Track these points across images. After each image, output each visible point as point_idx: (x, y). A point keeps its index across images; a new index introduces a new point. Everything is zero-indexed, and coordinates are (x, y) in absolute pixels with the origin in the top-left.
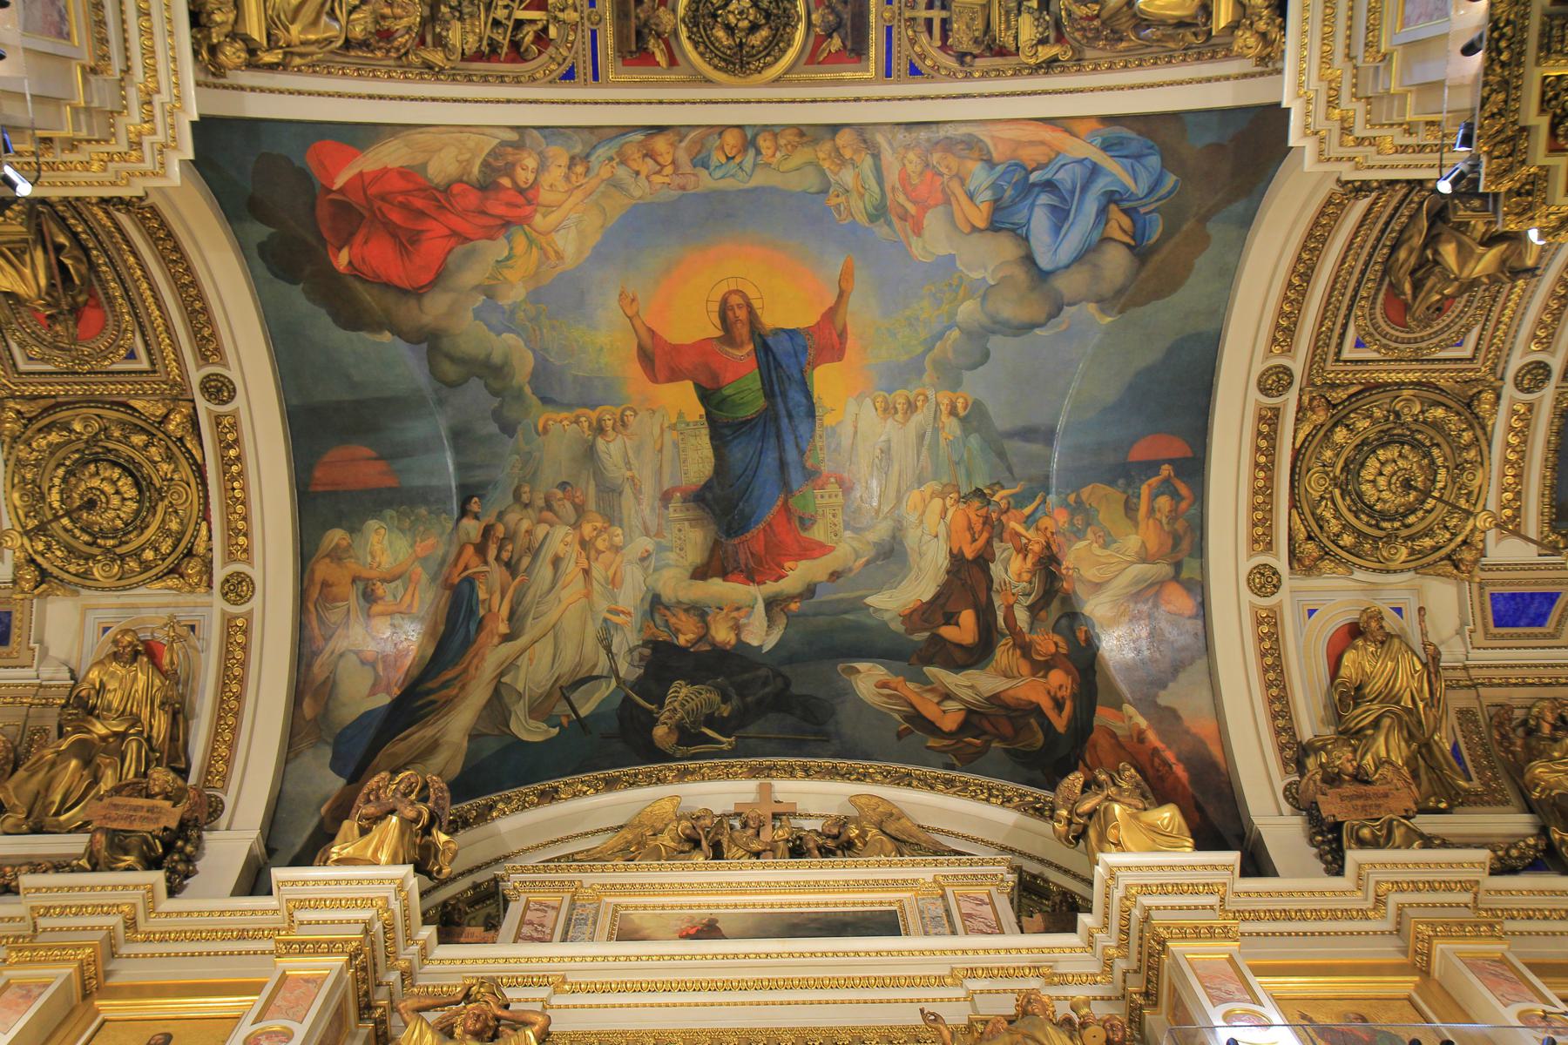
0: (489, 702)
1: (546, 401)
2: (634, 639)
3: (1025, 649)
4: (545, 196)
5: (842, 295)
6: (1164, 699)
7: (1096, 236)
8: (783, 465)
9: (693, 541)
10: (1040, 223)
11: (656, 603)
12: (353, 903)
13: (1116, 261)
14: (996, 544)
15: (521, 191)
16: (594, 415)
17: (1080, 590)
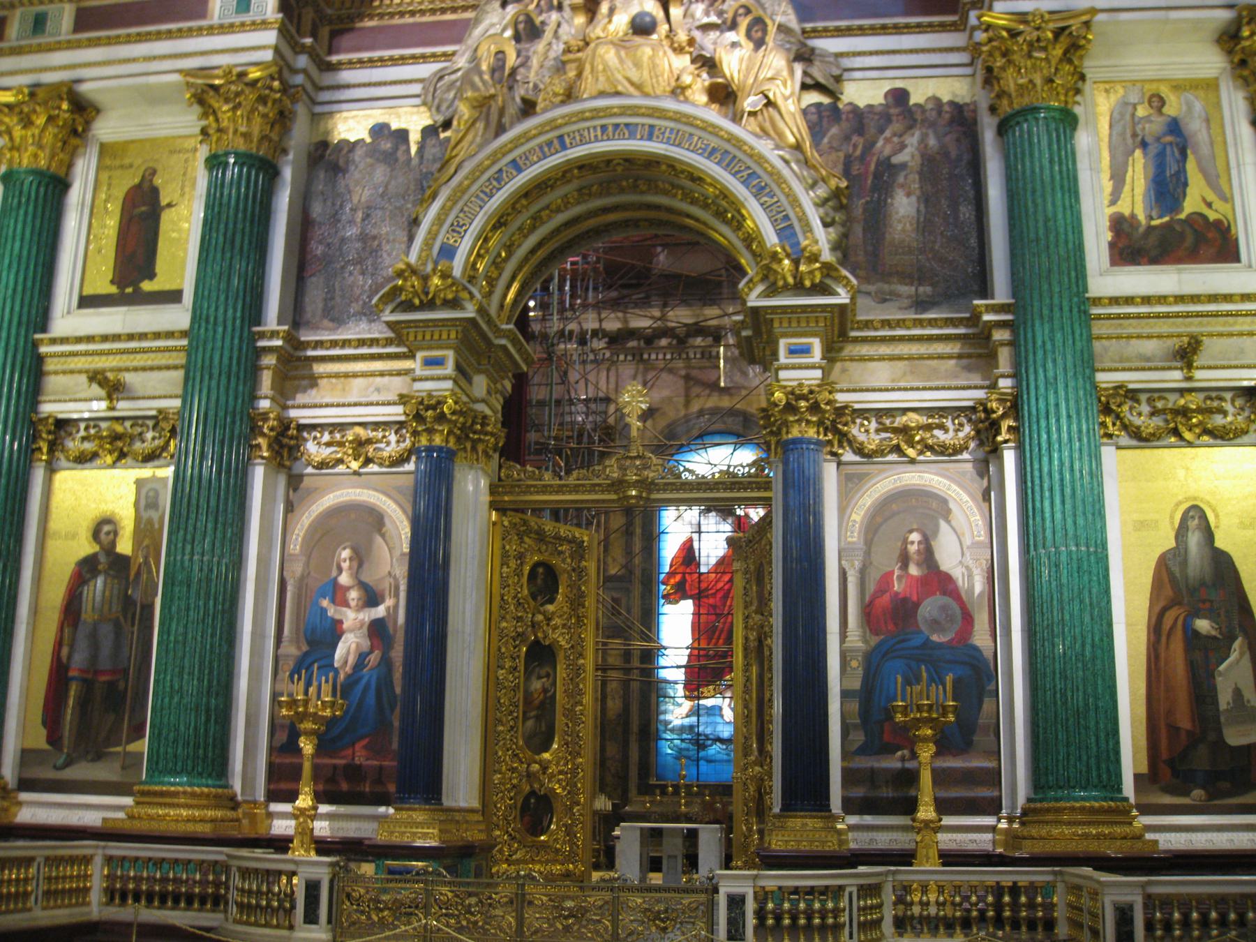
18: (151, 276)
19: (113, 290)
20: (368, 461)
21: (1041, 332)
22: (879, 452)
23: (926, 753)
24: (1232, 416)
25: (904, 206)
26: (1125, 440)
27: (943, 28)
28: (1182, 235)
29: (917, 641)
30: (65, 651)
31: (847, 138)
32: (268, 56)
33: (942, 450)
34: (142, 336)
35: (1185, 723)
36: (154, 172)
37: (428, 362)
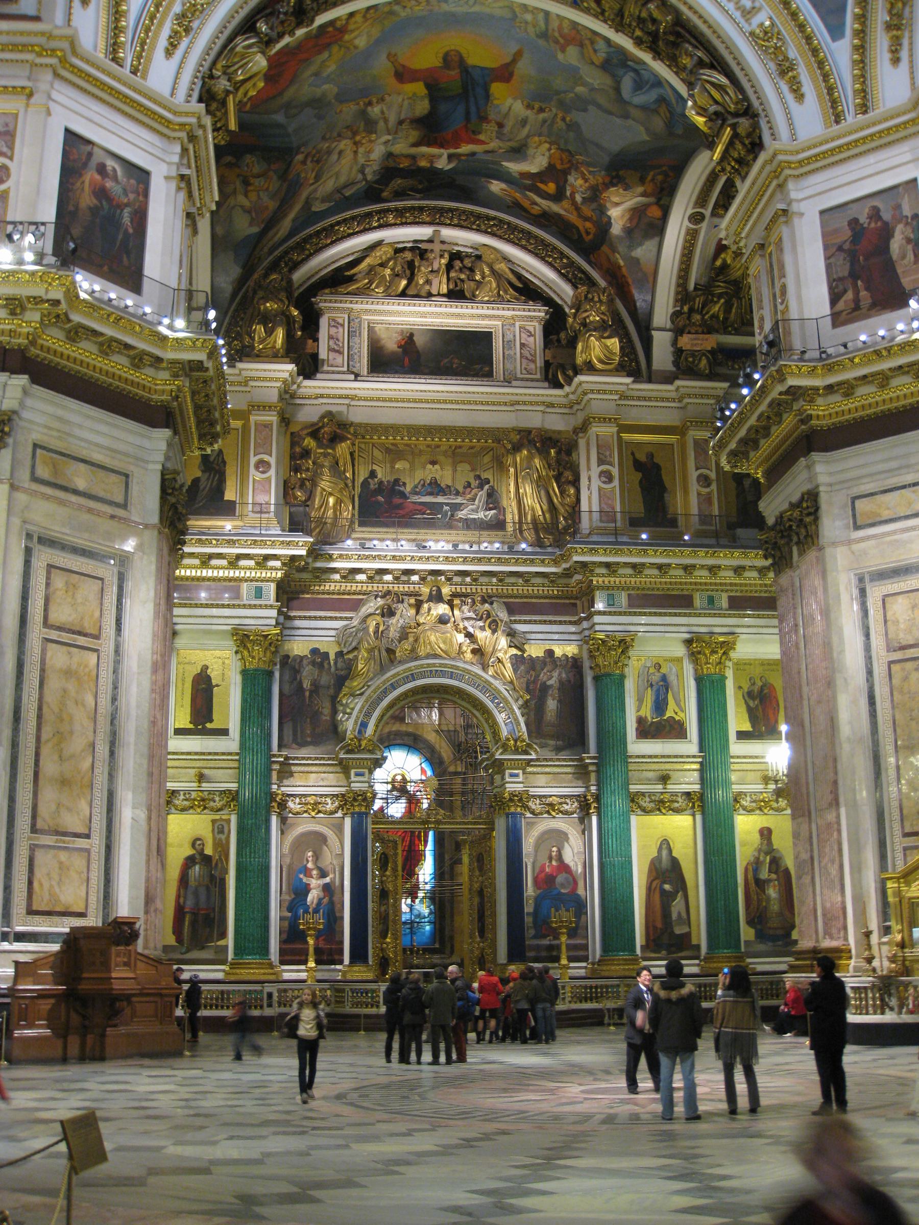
0: (302, 208)
1: (341, 102)
2: (376, 167)
3: (577, 209)
4: (351, 27)
5: (514, 61)
6: (634, 254)
7: (653, 107)
8: (468, 114)
9: (414, 135)
10: (627, 83)
11: (390, 155)
12: (271, 379)
13: (658, 124)
14: (573, 173)
15: (336, 29)
16: (367, 100)
17: (608, 205)
18: (211, 721)
19: (191, 726)
20: (319, 812)
21: (610, 770)
22: (541, 813)
23: (564, 939)
24: (681, 802)
25: (552, 704)
26: (640, 812)
27: (571, 623)
28: (664, 726)
29: (555, 892)
30: (182, 900)
31: (528, 672)
32: (273, 622)
33: (566, 813)
34: (216, 754)
35: (659, 925)
36: (207, 668)
37: (357, 775)
